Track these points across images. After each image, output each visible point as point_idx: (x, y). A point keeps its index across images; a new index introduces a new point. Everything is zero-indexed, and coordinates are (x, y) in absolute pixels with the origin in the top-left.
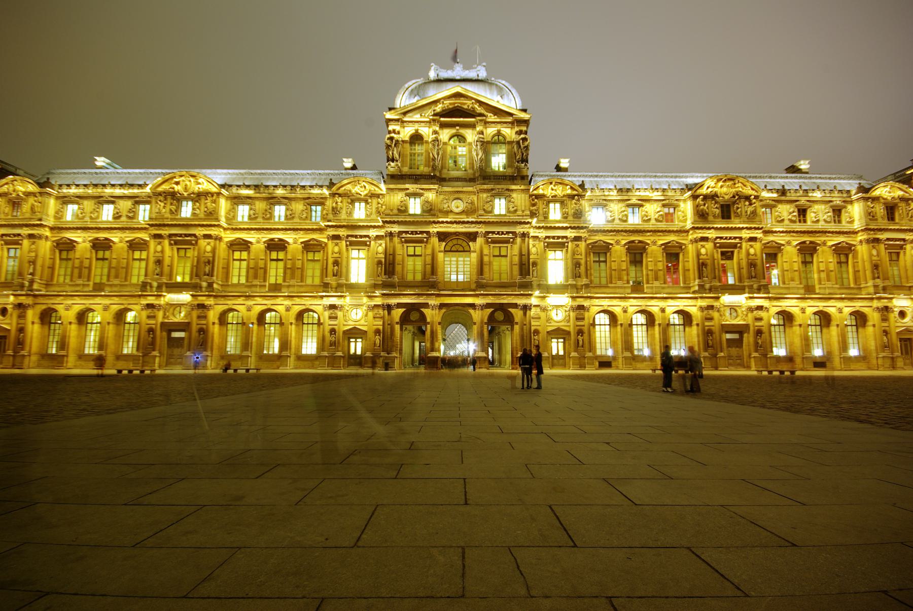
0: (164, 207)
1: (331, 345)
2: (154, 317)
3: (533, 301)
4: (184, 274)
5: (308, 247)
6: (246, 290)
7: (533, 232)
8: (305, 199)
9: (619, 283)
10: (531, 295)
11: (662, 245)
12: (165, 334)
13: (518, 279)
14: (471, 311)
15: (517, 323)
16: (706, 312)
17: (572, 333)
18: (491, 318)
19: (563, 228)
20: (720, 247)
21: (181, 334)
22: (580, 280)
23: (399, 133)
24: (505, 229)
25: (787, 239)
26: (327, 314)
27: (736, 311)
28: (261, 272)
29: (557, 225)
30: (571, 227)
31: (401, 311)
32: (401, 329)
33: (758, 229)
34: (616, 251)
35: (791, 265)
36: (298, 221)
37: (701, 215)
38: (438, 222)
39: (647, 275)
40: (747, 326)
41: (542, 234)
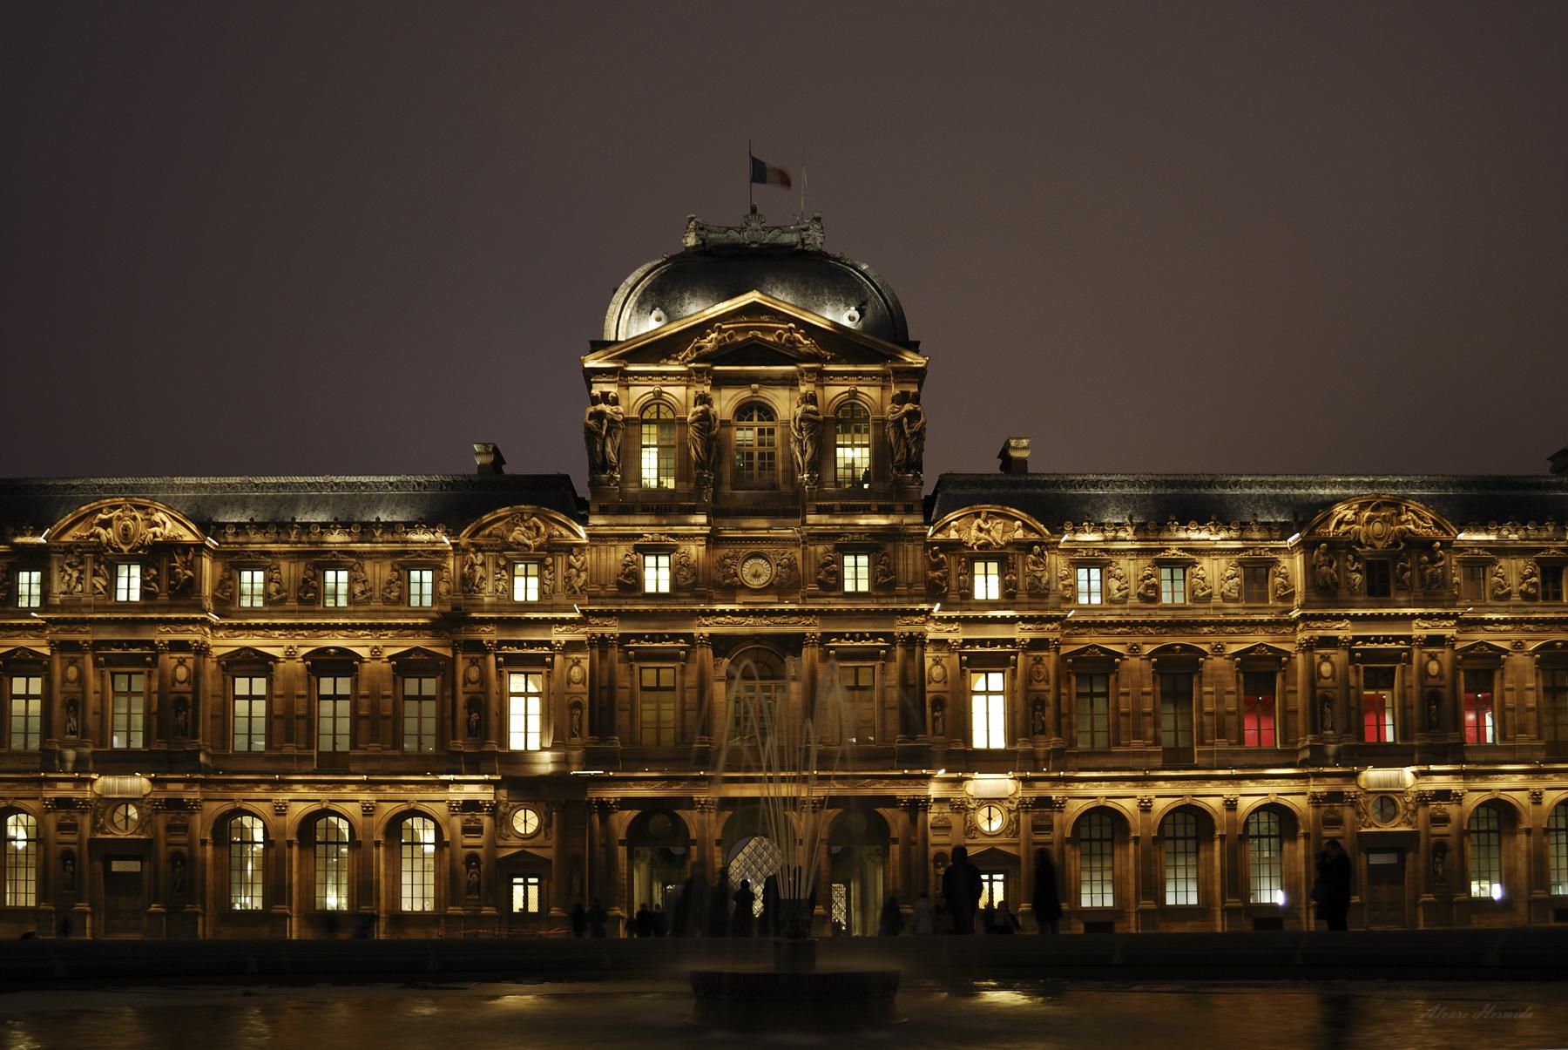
0: (79, 580)
1: (470, 890)
2: (73, 827)
3: (934, 790)
4: (129, 732)
6: (268, 766)
7: (932, 632)
8: (393, 554)
9: (1137, 745)
10: (928, 778)
11: (1236, 654)
12: (98, 864)
13: (898, 741)
14: (793, 816)
15: (895, 841)
16: (1325, 807)
17: (1023, 860)
18: (839, 832)
19: (1003, 620)
20: (1361, 660)
21: (134, 866)
22: (1041, 737)
23: (615, 401)
24: (867, 628)
25: (1515, 636)
26: (457, 822)
27: (1394, 803)
29: (991, 614)
30: (1023, 619)
31: (629, 815)
32: (631, 856)
33: (1447, 617)
34: (1130, 670)
35: (1521, 696)
36: (381, 606)
37: (1324, 590)
38: (713, 613)
39: (1201, 725)
40: (1413, 836)
41: (956, 635)
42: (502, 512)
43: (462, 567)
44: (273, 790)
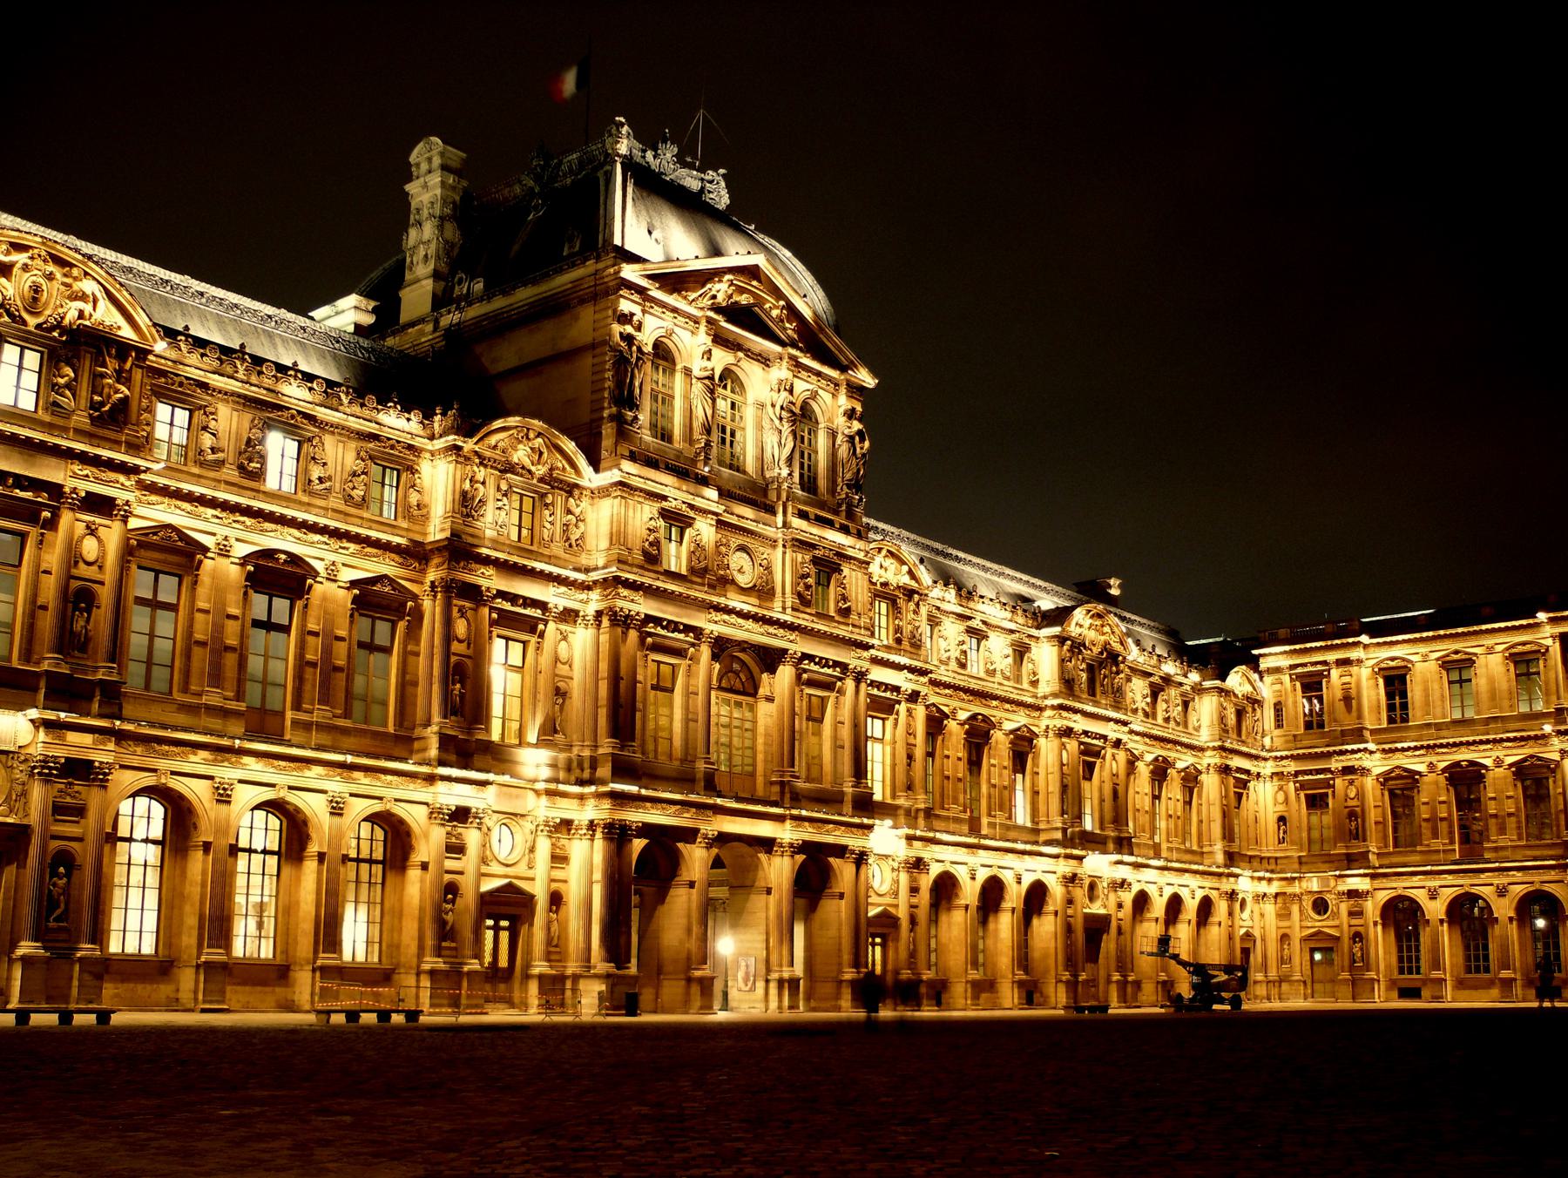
5: (371, 599)
28: (231, 660)
42: (513, 421)
43: (463, 480)
44: (215, 762)
